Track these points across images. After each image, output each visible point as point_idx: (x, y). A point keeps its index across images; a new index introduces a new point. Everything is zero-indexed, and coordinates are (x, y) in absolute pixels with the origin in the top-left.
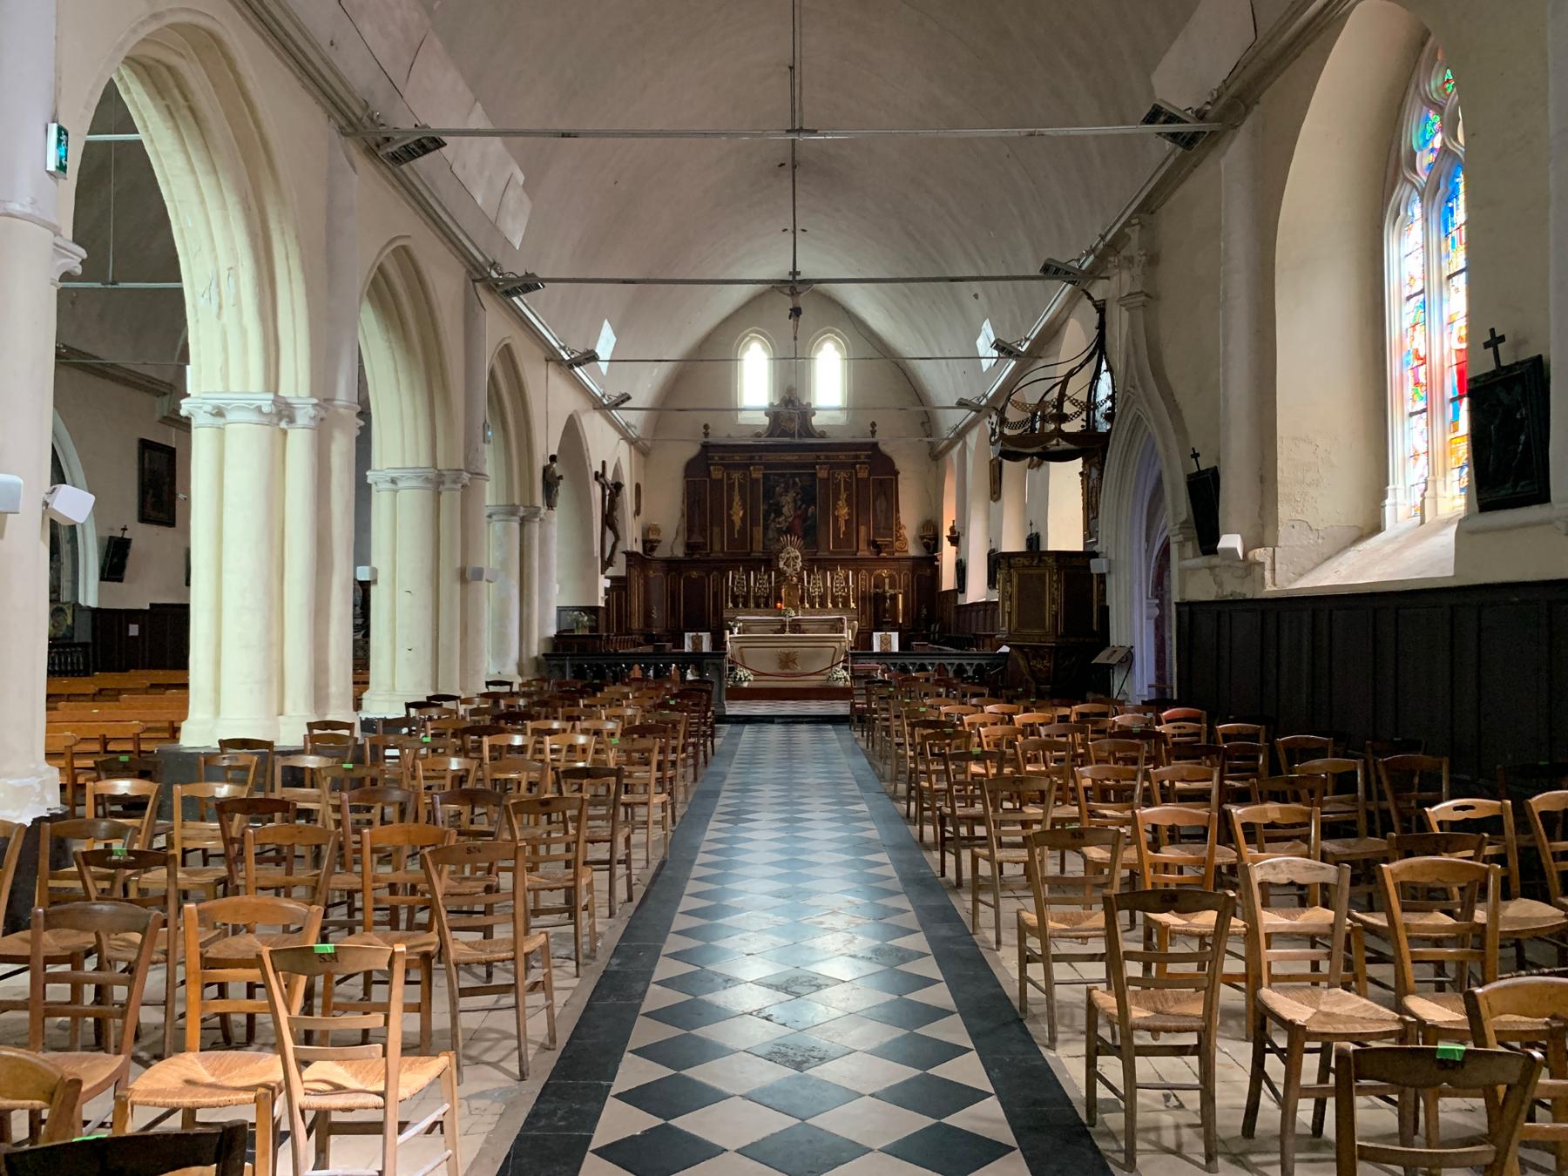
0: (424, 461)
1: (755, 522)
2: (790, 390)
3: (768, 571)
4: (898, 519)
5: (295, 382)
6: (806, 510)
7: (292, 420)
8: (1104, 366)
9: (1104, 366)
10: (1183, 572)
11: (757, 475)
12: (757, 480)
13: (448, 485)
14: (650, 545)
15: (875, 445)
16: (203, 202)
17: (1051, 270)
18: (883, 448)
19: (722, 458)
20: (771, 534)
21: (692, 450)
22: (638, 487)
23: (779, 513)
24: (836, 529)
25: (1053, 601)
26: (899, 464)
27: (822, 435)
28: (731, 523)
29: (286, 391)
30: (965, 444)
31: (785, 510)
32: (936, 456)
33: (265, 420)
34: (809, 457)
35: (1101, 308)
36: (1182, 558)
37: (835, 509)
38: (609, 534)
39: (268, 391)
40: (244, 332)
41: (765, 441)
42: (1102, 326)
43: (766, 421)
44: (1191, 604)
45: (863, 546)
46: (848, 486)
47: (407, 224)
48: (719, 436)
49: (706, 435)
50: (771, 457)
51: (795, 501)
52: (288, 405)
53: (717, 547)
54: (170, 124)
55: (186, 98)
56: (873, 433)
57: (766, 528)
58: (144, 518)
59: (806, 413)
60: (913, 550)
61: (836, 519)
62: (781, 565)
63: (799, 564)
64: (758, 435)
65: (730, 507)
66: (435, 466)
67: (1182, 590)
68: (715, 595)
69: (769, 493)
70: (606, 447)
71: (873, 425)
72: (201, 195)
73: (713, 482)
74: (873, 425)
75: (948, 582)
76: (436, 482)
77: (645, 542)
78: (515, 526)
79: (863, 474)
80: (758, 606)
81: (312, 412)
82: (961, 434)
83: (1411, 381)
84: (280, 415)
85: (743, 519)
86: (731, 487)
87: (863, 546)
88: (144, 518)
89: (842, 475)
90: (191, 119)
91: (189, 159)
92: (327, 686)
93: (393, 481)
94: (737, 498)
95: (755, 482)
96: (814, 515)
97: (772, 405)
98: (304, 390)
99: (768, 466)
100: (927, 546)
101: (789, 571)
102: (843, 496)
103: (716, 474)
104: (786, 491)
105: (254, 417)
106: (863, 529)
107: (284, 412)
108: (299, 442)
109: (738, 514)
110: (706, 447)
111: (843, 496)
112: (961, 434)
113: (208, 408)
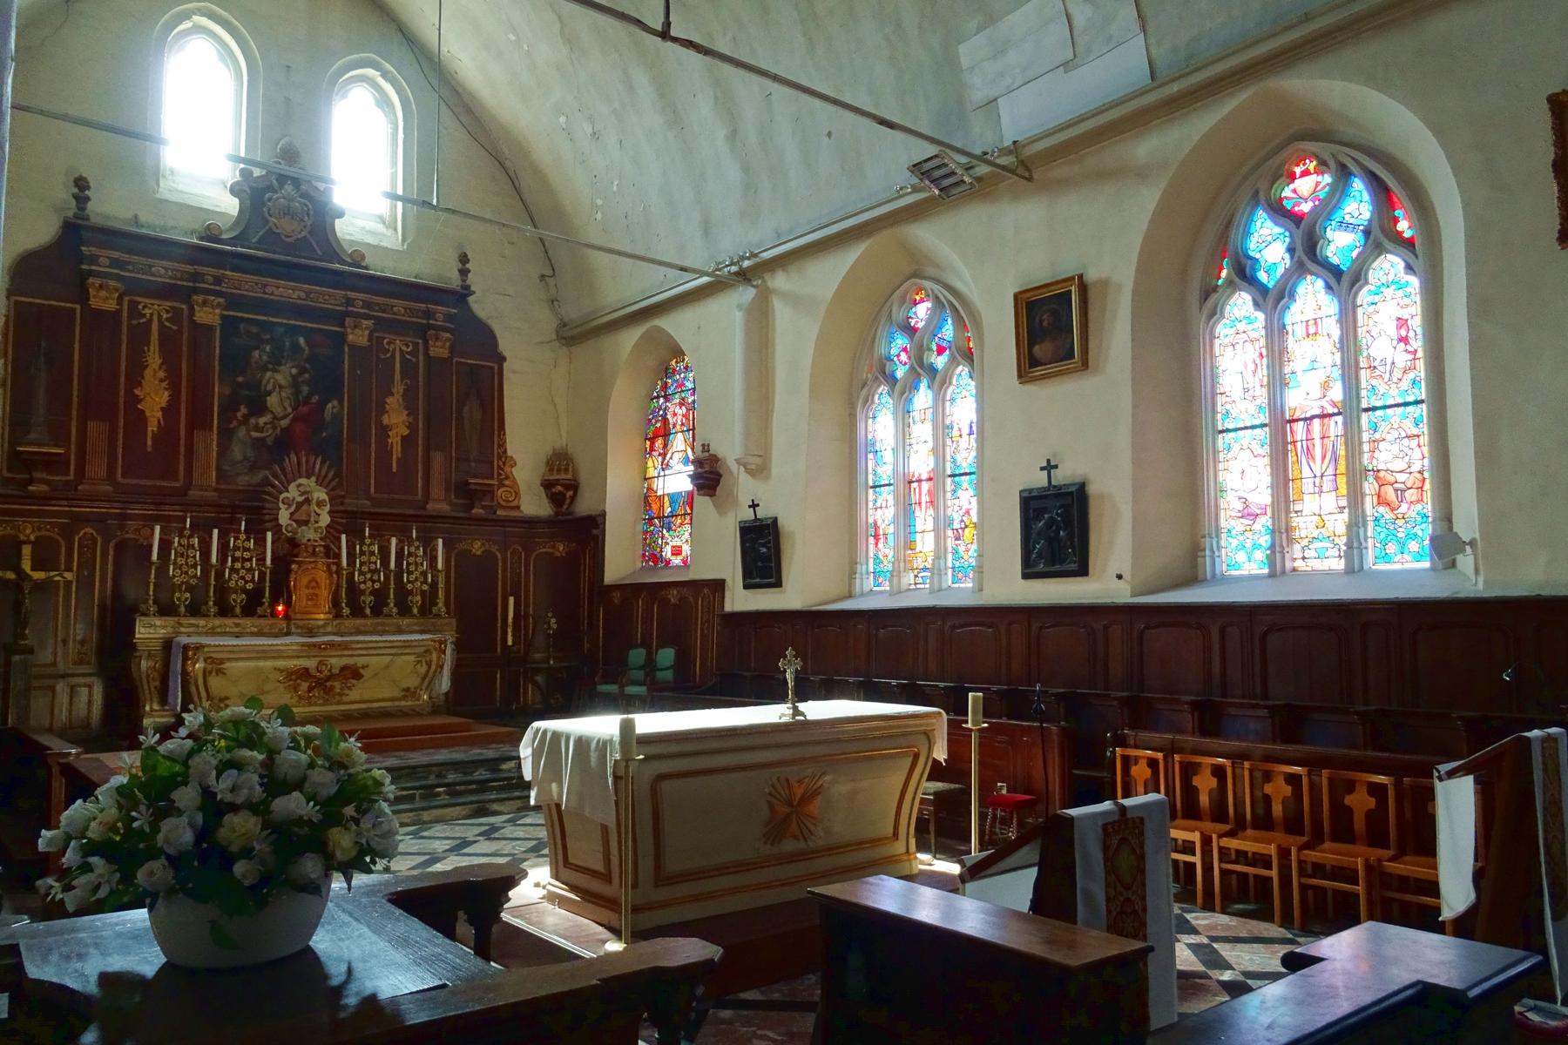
1: (199, 420)
3: (256, 531)
4: (502, 444)
6: (322, 405)
11: (208, 315)
12: (209, 328)
15: (461, 296)
18: (482, 305)
19: (116, 263)
20: (237, 452)
23: (259, 407)
24: (384, 451)
26: (504, 346)
27: (357, 259)
30: (764, 297)
31: (272, 401)
32: (578, 334)
34: (330, 298)
37: (382, 409)
46: (409, 370)
50: (247, 285)
51: (295, 384)
53: (97, 468)
56: (464, 272)
57: (226, 435)
60: (534, 504)
61: (384, 431)
62: (284, 517)
69: (236, 361)
71: (464, 259)
73: (96, 318)
74: (464, 259)
79: (439, 350)
80: (225, 611)
85: (170, 411)
86: (140, 336)
87: (437, 491)
89: (398, 345)
94: (154, 359)
96: (337, 417)
99: (234, 302)
102: (398, 388)
103: (104, 301)
104: (276, 361)
106: (438, 459)
109: (154, 398)
111: (398, 388)
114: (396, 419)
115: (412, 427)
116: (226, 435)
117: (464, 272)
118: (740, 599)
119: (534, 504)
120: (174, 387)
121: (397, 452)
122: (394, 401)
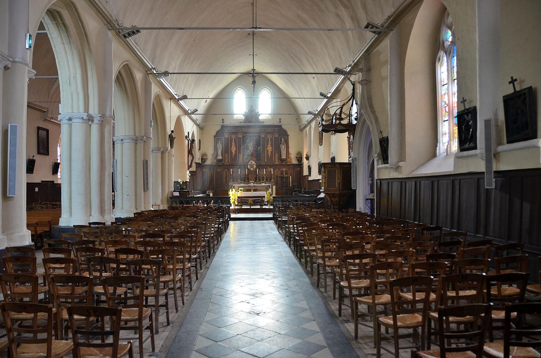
0: (132, 134)
2: (252, 107)
5: (94, 110)
7: (93, 121)
8: (354, 102)
9: (354, 102)
10: (378, 169)
11: (240, 136)
13: (139, 141)
14: (203, 160)
15: (281, 126)
16: (66, 53)
17: (338, 71)
18: (283, 127)
21: (219, 128)
22: (200, 140)
24: (268, 155)
25: (338, 179)
26: (289, 133)
27: (263, 122)
28: (232, 153)
29: (91, 112)
30: (311, 126)
31: (250, 148)
32: (302, 130)
33: (85, 122)
35: (354, 85)
36: (378, 165)
37: (267, 147)
38: (190, 156)
39: (85, 112)
40: (78, 94)
41: (243, 124)
42: (354, 90)
43: (243, 118)
44: (380, 180)
45: (277, 160)
46: (271, 140)
47: (126, 56)
48: (227, 123)
49: (223, 122)
52: (92, 116)
53: (227, 161)
54: (57, 29)
55: (62, 21)
56: (280, 122)
57: (243, 155)
58: (39, 153)
59: (258, 115)
60: (294, 162)
61: (267, 151)
62: (249, 167)
63: (255, 167)
64: (240, 123)
65: (231, 147)
66: (135, 135)
67: (378, 176)
68: (226, 177)
70: (189, 127)
71: (280, 119)
72: (66, 51)
74: (280, 119)
75: (306, 172)
76: (136, 140)
77: (202, 159)
78: (159, 155)
81: (99, 119)
82: (310, 122)
83: (444, 111)
84: (89, 120)
85: (236, 151)
88: (39, 153)
90: (63, 28)
91: (62, 39)
92: (105, 207)
93: (122, 140)
94: (233, 144)
95: (239, 138)
97: (245, 112)
98: (96, 112)
100: (298, 160)
101: (252, 169)
102: (270, 143)
105: (81, 121)
107: (90, 119)
108: (95, 129)
110: (223, 127)
111: (270, 143)
112: (310, 122)
113: (67, 118)
114: (270, 148)
115: (272, 150)
116: (243, 155)
117: (280, 122)
118: (310, 179)
119: (294, 162)
120: (236, 148)
121: (270, 154)
122: (269, 146)
